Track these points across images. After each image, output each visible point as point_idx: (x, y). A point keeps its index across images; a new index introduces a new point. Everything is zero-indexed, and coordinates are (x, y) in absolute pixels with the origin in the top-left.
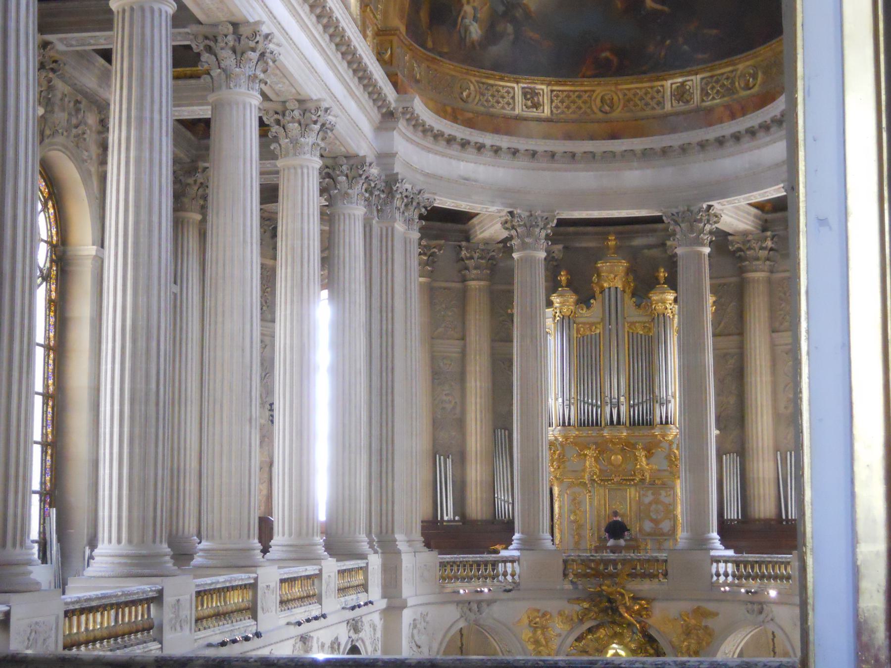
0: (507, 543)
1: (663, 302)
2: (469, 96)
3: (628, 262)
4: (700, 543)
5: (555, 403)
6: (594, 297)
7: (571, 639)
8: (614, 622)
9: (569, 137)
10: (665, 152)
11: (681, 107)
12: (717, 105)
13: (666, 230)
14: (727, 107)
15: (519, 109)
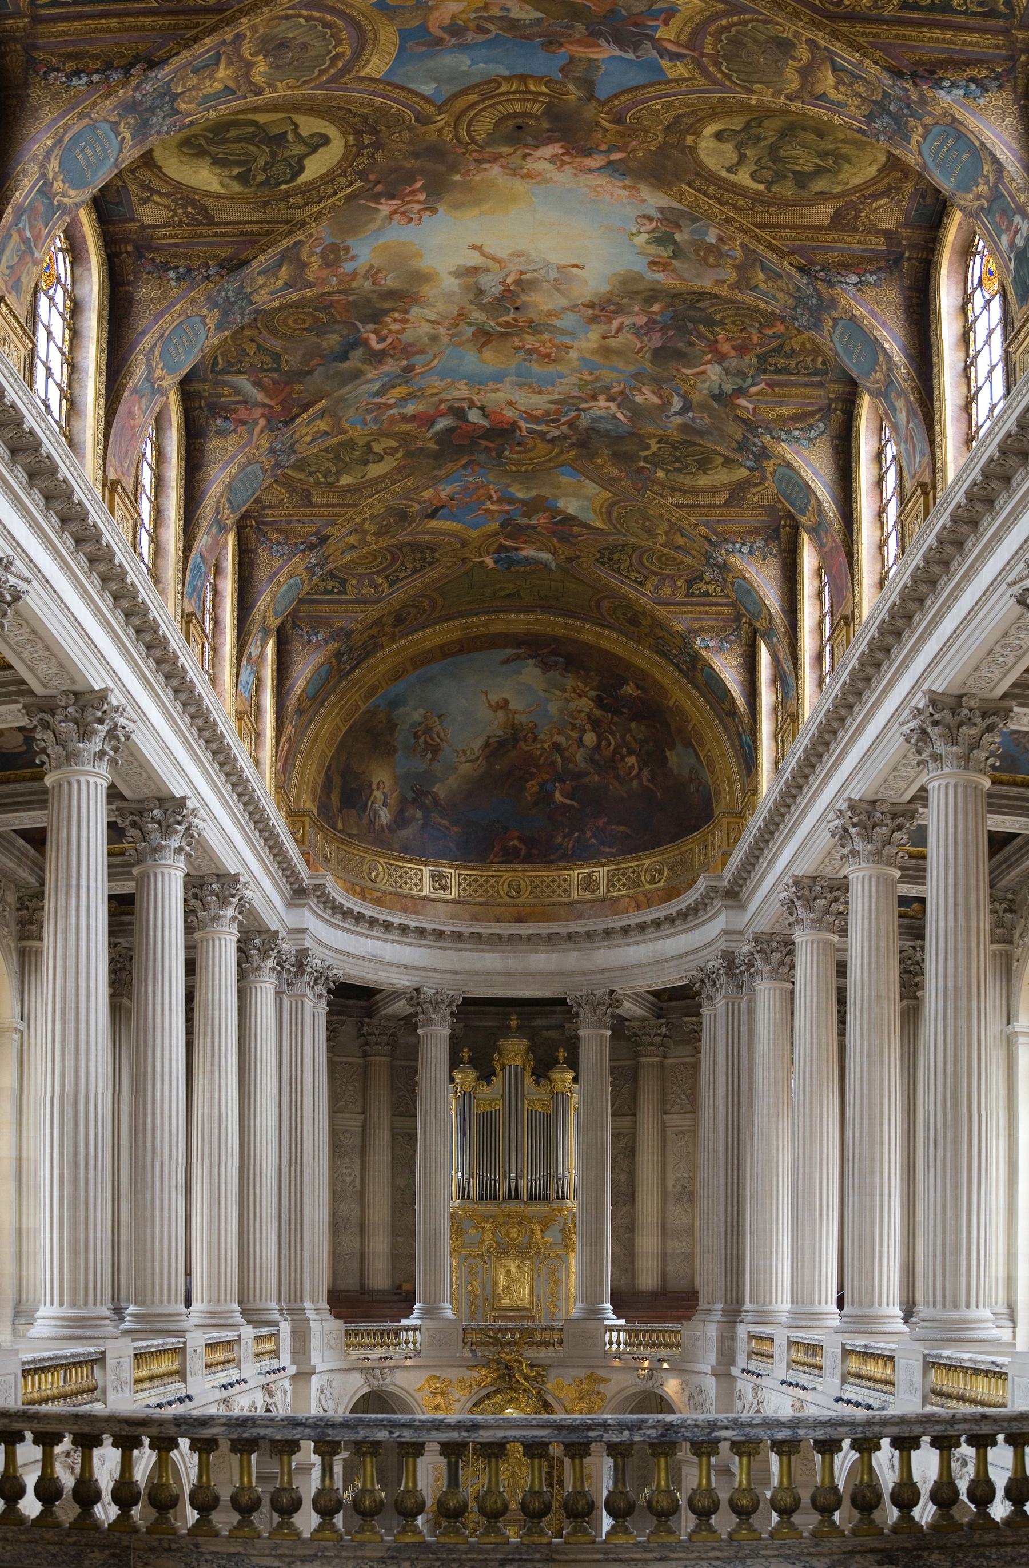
0: (408, 1313)
1: (563, 1081)
2: (377, 876)
3: (529, 1040)
4: (594, 1313)
5: (456, 1176)
6: (494, 1074)
7: (469, 1405)
8: (511, 1388)
9: (475, 918)
10: (570, 936)
11: (587, 896)
12: (623, 896)
13: (569, 1012)
14: (633, 897)
15: (427, 890)
